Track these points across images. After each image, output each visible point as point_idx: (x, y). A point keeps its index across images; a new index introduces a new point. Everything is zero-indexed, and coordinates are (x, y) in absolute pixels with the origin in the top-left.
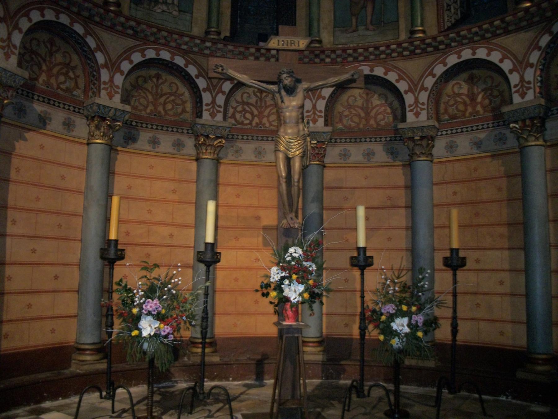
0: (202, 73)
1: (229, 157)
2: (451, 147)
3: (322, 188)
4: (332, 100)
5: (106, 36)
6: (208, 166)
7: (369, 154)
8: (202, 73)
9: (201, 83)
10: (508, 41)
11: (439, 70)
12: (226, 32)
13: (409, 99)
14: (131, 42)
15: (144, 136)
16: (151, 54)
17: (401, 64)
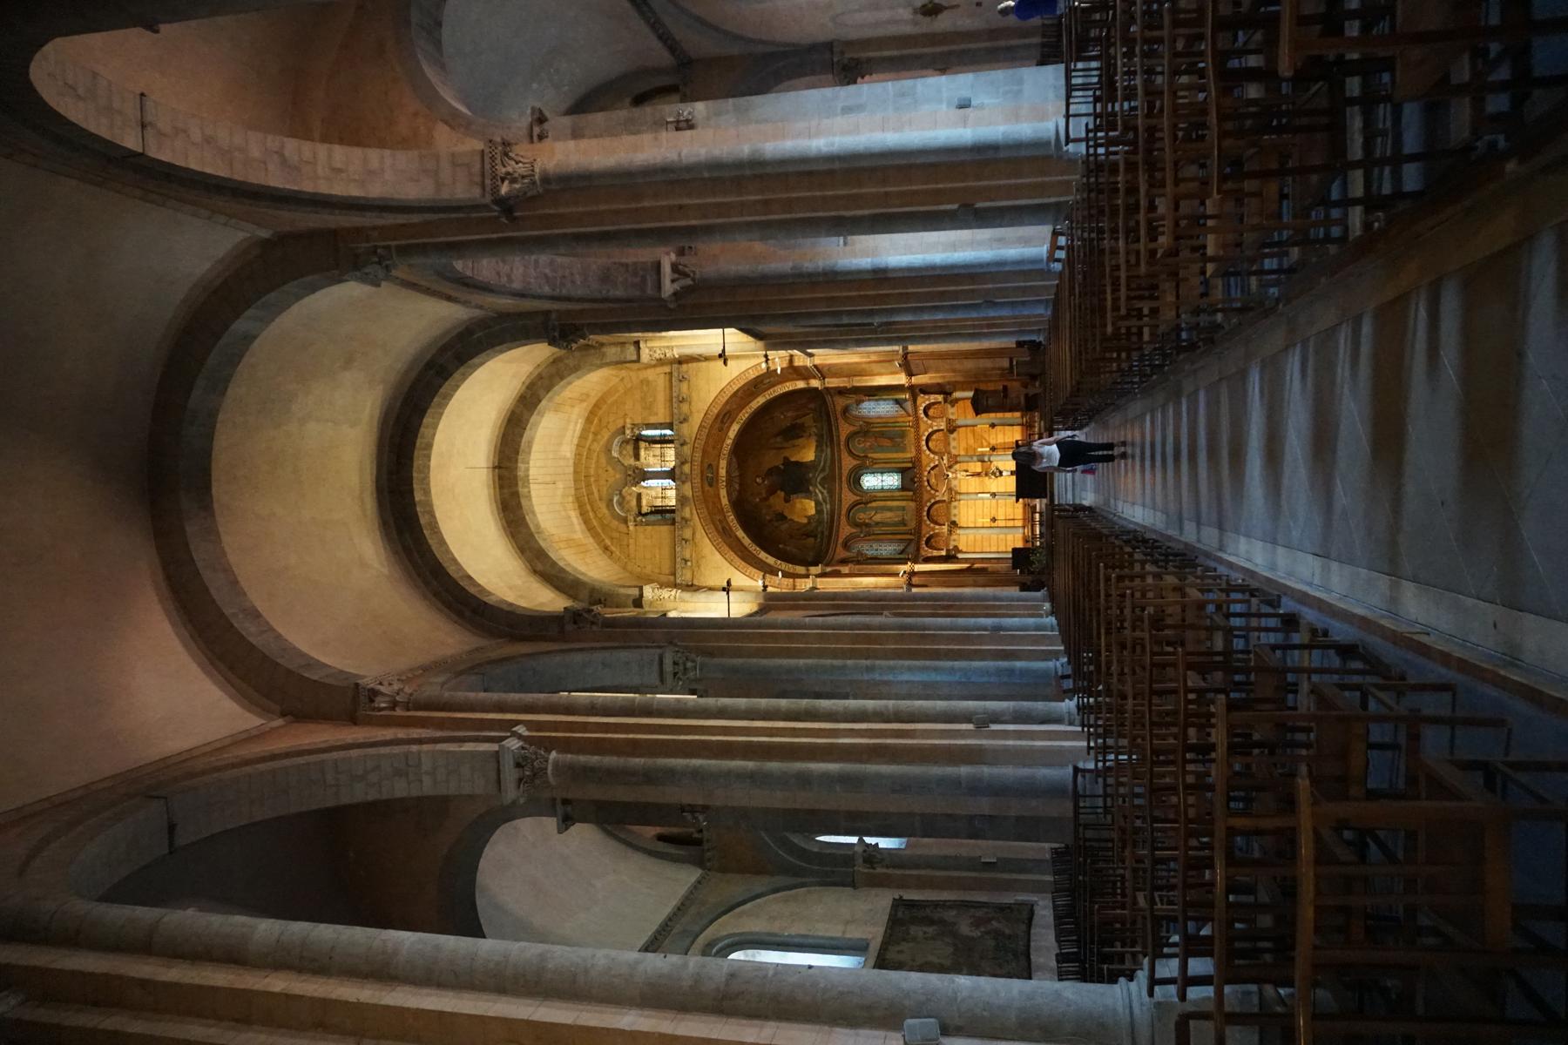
0: (929, 500)
1: (958, 489)
2: (952, 414)
3: (966, 455)
4: (933, 453)
5: (923, 532)
6: (962, 497)
7: (954, 439)
8: (929, 500)
9: (933, 501)
10: (918, 402)
11: (925, 419)
12: (911, 493)
13: (935, 428)
14: (924, 526)
15: (953, 519)
16: (926, 518)
17: (922, 430)
